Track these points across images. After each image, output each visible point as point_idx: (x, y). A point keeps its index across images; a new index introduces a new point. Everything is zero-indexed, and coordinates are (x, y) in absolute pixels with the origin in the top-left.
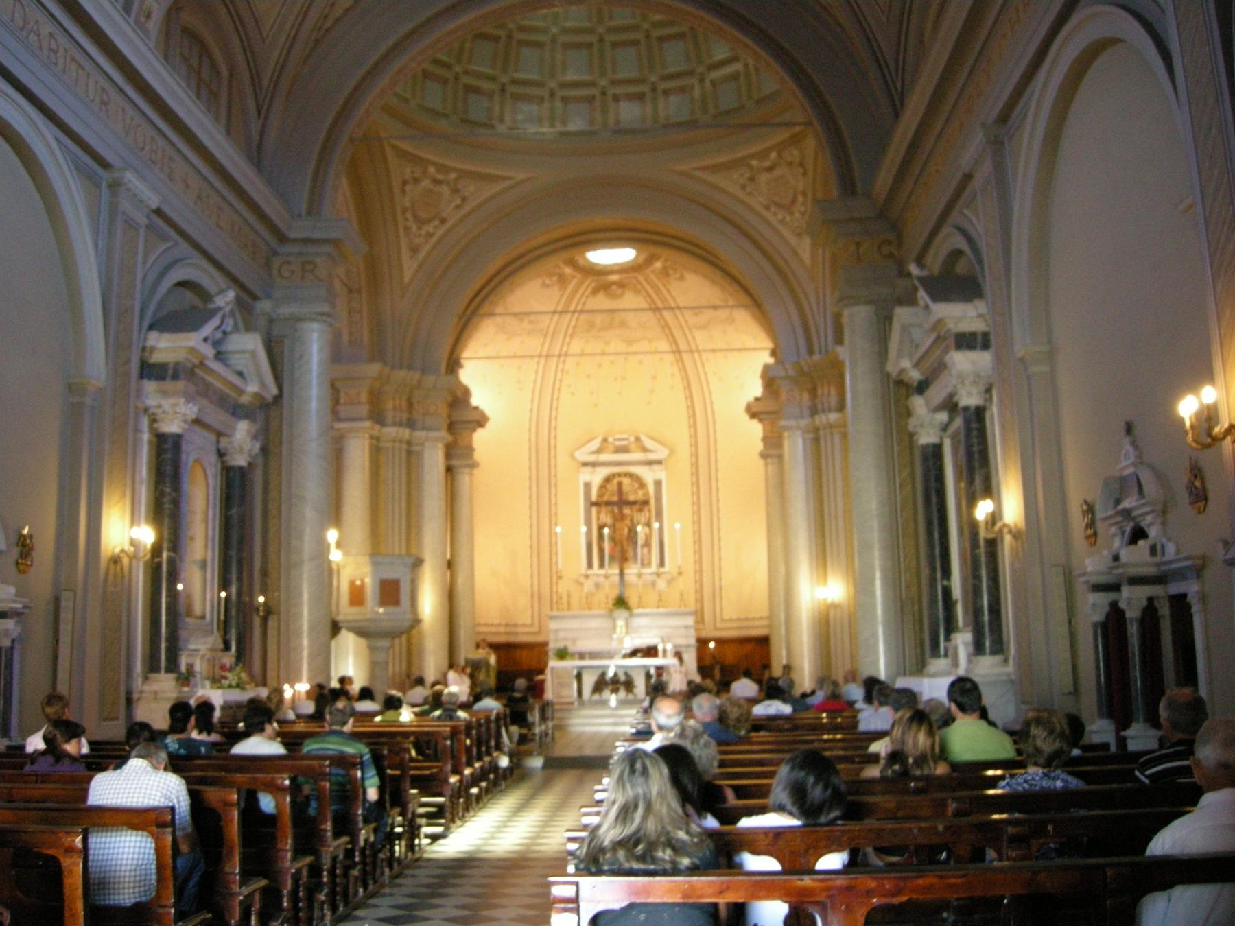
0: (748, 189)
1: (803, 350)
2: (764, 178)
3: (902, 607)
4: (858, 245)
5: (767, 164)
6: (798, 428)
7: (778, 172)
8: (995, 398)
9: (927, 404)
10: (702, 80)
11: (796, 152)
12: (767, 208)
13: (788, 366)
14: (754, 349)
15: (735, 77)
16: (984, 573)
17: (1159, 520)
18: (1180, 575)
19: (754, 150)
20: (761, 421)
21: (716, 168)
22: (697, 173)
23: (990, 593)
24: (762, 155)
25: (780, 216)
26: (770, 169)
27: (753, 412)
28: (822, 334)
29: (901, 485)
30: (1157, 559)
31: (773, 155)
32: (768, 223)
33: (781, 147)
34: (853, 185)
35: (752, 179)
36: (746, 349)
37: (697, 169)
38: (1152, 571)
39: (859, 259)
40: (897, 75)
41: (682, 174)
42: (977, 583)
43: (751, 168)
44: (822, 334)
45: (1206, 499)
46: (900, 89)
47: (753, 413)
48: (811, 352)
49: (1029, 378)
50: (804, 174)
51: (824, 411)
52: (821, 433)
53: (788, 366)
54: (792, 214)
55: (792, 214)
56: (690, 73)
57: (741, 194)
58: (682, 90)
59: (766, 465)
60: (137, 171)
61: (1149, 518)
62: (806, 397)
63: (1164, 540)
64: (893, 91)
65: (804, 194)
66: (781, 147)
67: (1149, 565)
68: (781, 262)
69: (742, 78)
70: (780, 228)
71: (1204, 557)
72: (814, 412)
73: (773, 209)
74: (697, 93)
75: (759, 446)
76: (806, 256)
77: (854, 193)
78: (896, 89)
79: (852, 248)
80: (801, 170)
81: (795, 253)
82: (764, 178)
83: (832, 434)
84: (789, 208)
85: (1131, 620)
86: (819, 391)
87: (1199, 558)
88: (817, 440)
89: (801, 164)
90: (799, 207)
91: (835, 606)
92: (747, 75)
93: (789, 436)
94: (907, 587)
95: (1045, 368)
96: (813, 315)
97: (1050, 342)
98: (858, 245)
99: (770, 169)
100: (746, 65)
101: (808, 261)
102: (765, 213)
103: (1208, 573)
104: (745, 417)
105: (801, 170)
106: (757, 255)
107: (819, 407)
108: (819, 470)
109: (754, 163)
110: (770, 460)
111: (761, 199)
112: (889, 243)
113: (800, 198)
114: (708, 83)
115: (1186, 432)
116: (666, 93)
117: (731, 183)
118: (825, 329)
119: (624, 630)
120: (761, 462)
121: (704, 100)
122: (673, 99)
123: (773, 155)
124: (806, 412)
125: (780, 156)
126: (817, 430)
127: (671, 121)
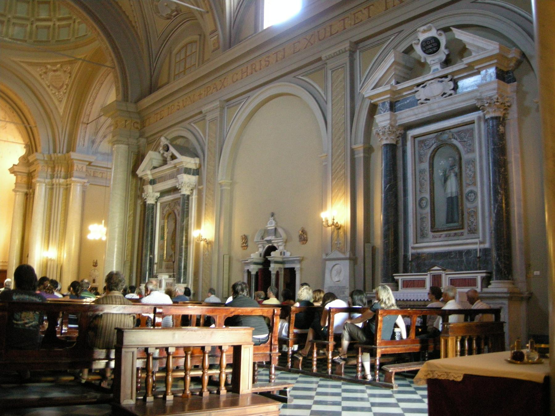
0: (42, 77)
1: (51, 151)
2: (51, 74)
3: (124, 264)
4: (126, 121)
5: (55, 68)
6: (44, 182)
7: (58, 73)
8: (194, 193)
9: (153, 189)
10: (32, 24)
11: (69, 68)
12: (49, 87)
13: (45, 156)
14: (13, 142)
15: (48, 27)
16: (183, 254)
17: (284, 244)
18: (293, 262)
19: (51, 61)
20: (15, 175)
21: (30, 64)
22: (22, 64)
23: (185, 262)
24: (54, 64)
25: (53, 92)
26: (54, 71)
27: (12, 171)
28: (62, 143)
29: (129, 217)
30: (282, 256)
31: (59, 66)
32: (48, 94)
33: (63, 64)
34: (127, 97)
35: (45, 73)
36: (8, 141)
37: (23, 62)
38: (280, 260)
39: (125, 127)
40: (155, 60)
41: (14, 61)
42: (180, 257)
43: (47, 68)
44: (62, 143)
45: (307, 240)
46: (154, 66)
47: (12, 171)
48: (55, 152)
49: (222, 191)
50: (70, 77)
51: (57, 177)
52: (55, 186)
53: (45, 156)
54: (59, 92)
55: (59, 92)
56: (28, 19)
57: (39, 78)
58: (22, 25)
59: (16, 195)
60: (205, 105)
61: (280, 244)
62: (50, 170)
63: (285, 251)
64: (152, 67)
65: (67, 85)
66: (63, 64)
67: (279, 258)
68: (49, 110)
69: (51, 29)
70: (53, 97)
71: (303, 257)
72: (52, 177)
73: (51, 87)
74: (28, 28)
75: (13, 187)
76: (61, 111)
77: (127, 101)
78: (153, 66)
79: (123, 122)
80: (69, 75)
81: (57, 109)
82: (51, 74)
83: (60, 188)
84: (59, 89)
85: (273, 274)
86: (56, 169)
87: (301, 257)
88: (52, 189)
89: (70, 73)
90: (63, 90)
91: (51, 260)
92: (54, 29)
93: (39, 185)
94: (127, 256)
95: (229, 188)
96: (59, 135)
97: (232, 179)
98: (126, 121)
99: (54, 71)
100: (54, 24)
101: (61, 114)
102: (47, 89)
103: (304, 263)
104: (9, 172)
105: (69, 75)
106: (39, 105)
107: (56, 175)
108: (51, 202)
109: (49, 66)
110: (18, 193)
111: (47, 82)
112: (137, 123)
113: (65, 87)
114: (34, 26)
115: (323, 222)
116: (14, 24)
117: (36, 72)
118: (64, 142)
119: (280, 273)
120: (13, 193)
121: (31, 33)
122: (16, 28)
123: (59, 66)
124: (49, 176)
125: (61, 67)
126: (53, 185)
127: (13, 37)
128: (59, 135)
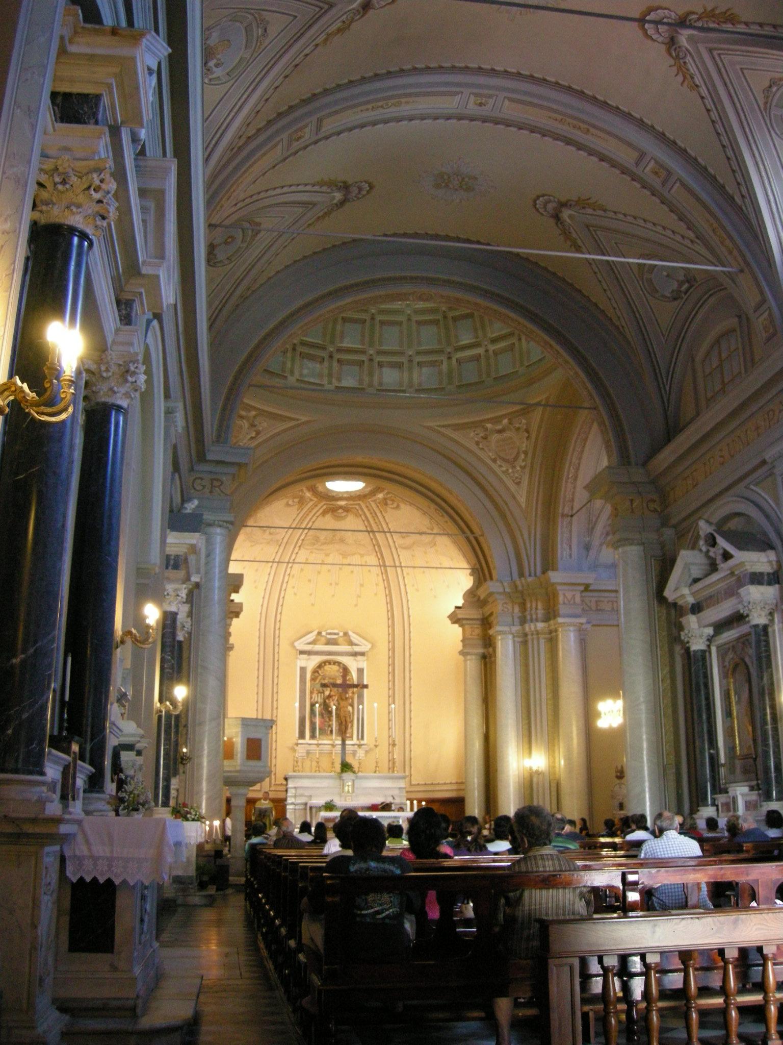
0: (481, 446)
3: (664, 770)
4: (632, 501)
5: (499, 427)
7: (507, 434)
8: (776, 620)
10: (450, 358)
11: (524, 421)
12: (494, 461)
13: (505, 584)
15: (477, 358)
16: (771, 742)
20: (460, 626)
21: (457, 427)
22: (443, 430)
24: (496, 420)
25: (504, 469)
26: (500, 432)
27: (455, 618)
29: (662, 680)
31: (505, 421)
32: (494, 472)
34: (628, 457)
37: (443, 426)
39: (632, 511)
40: (667, 380)
43: (486, 429)
47: (455, 618)
48: (521, 574)
50: (528, 438)
51: (532, 621)
52: (529, 637)
53: (505, 584)
54: (514, 467)
55: (514, 467)
56: (440, 352)
57: (473, 447)
58: (433, 364)
59: (465, 661)
62: (517, 609)
64: (663, 391)
65: (526, 453)
66: (511, 417)
69: (483, 361)
72: (523, 621)
74: (445, 367)
75: (460, 646)
76: (522, 500)
77: (629, 464)
79: (628, 503)
81: (514, 497)
82: (495, 437)
83: (538, 639)
84: (512, 462)
86: (528, 605)
88: (525, 643)
89: (527, 431)
90: (520, 462)
91: (538, 773)
92: (487, 358)
93: (501, 639)
96: (525, 544)
98: (632, 501)
100: (487, 351)
101: (524, 505)
107: (528, 617)
108: (526, 665)
109: (489, 426)
110: (469, 657)
112: (654, 501)
114: (454, 361)
117: (468, 439)
120: (461, 658)
122: (424, 370)
123: (505, 421)
124: (517, 621)
126: (526, 635)
128: (525, 544)
